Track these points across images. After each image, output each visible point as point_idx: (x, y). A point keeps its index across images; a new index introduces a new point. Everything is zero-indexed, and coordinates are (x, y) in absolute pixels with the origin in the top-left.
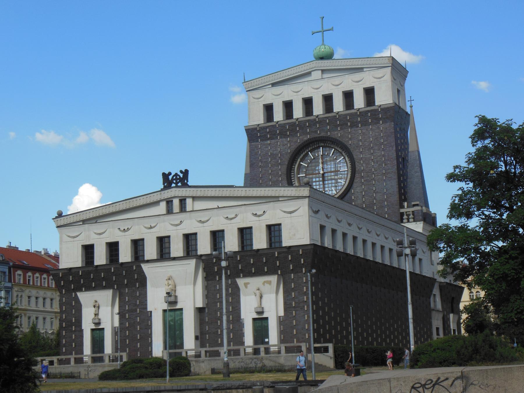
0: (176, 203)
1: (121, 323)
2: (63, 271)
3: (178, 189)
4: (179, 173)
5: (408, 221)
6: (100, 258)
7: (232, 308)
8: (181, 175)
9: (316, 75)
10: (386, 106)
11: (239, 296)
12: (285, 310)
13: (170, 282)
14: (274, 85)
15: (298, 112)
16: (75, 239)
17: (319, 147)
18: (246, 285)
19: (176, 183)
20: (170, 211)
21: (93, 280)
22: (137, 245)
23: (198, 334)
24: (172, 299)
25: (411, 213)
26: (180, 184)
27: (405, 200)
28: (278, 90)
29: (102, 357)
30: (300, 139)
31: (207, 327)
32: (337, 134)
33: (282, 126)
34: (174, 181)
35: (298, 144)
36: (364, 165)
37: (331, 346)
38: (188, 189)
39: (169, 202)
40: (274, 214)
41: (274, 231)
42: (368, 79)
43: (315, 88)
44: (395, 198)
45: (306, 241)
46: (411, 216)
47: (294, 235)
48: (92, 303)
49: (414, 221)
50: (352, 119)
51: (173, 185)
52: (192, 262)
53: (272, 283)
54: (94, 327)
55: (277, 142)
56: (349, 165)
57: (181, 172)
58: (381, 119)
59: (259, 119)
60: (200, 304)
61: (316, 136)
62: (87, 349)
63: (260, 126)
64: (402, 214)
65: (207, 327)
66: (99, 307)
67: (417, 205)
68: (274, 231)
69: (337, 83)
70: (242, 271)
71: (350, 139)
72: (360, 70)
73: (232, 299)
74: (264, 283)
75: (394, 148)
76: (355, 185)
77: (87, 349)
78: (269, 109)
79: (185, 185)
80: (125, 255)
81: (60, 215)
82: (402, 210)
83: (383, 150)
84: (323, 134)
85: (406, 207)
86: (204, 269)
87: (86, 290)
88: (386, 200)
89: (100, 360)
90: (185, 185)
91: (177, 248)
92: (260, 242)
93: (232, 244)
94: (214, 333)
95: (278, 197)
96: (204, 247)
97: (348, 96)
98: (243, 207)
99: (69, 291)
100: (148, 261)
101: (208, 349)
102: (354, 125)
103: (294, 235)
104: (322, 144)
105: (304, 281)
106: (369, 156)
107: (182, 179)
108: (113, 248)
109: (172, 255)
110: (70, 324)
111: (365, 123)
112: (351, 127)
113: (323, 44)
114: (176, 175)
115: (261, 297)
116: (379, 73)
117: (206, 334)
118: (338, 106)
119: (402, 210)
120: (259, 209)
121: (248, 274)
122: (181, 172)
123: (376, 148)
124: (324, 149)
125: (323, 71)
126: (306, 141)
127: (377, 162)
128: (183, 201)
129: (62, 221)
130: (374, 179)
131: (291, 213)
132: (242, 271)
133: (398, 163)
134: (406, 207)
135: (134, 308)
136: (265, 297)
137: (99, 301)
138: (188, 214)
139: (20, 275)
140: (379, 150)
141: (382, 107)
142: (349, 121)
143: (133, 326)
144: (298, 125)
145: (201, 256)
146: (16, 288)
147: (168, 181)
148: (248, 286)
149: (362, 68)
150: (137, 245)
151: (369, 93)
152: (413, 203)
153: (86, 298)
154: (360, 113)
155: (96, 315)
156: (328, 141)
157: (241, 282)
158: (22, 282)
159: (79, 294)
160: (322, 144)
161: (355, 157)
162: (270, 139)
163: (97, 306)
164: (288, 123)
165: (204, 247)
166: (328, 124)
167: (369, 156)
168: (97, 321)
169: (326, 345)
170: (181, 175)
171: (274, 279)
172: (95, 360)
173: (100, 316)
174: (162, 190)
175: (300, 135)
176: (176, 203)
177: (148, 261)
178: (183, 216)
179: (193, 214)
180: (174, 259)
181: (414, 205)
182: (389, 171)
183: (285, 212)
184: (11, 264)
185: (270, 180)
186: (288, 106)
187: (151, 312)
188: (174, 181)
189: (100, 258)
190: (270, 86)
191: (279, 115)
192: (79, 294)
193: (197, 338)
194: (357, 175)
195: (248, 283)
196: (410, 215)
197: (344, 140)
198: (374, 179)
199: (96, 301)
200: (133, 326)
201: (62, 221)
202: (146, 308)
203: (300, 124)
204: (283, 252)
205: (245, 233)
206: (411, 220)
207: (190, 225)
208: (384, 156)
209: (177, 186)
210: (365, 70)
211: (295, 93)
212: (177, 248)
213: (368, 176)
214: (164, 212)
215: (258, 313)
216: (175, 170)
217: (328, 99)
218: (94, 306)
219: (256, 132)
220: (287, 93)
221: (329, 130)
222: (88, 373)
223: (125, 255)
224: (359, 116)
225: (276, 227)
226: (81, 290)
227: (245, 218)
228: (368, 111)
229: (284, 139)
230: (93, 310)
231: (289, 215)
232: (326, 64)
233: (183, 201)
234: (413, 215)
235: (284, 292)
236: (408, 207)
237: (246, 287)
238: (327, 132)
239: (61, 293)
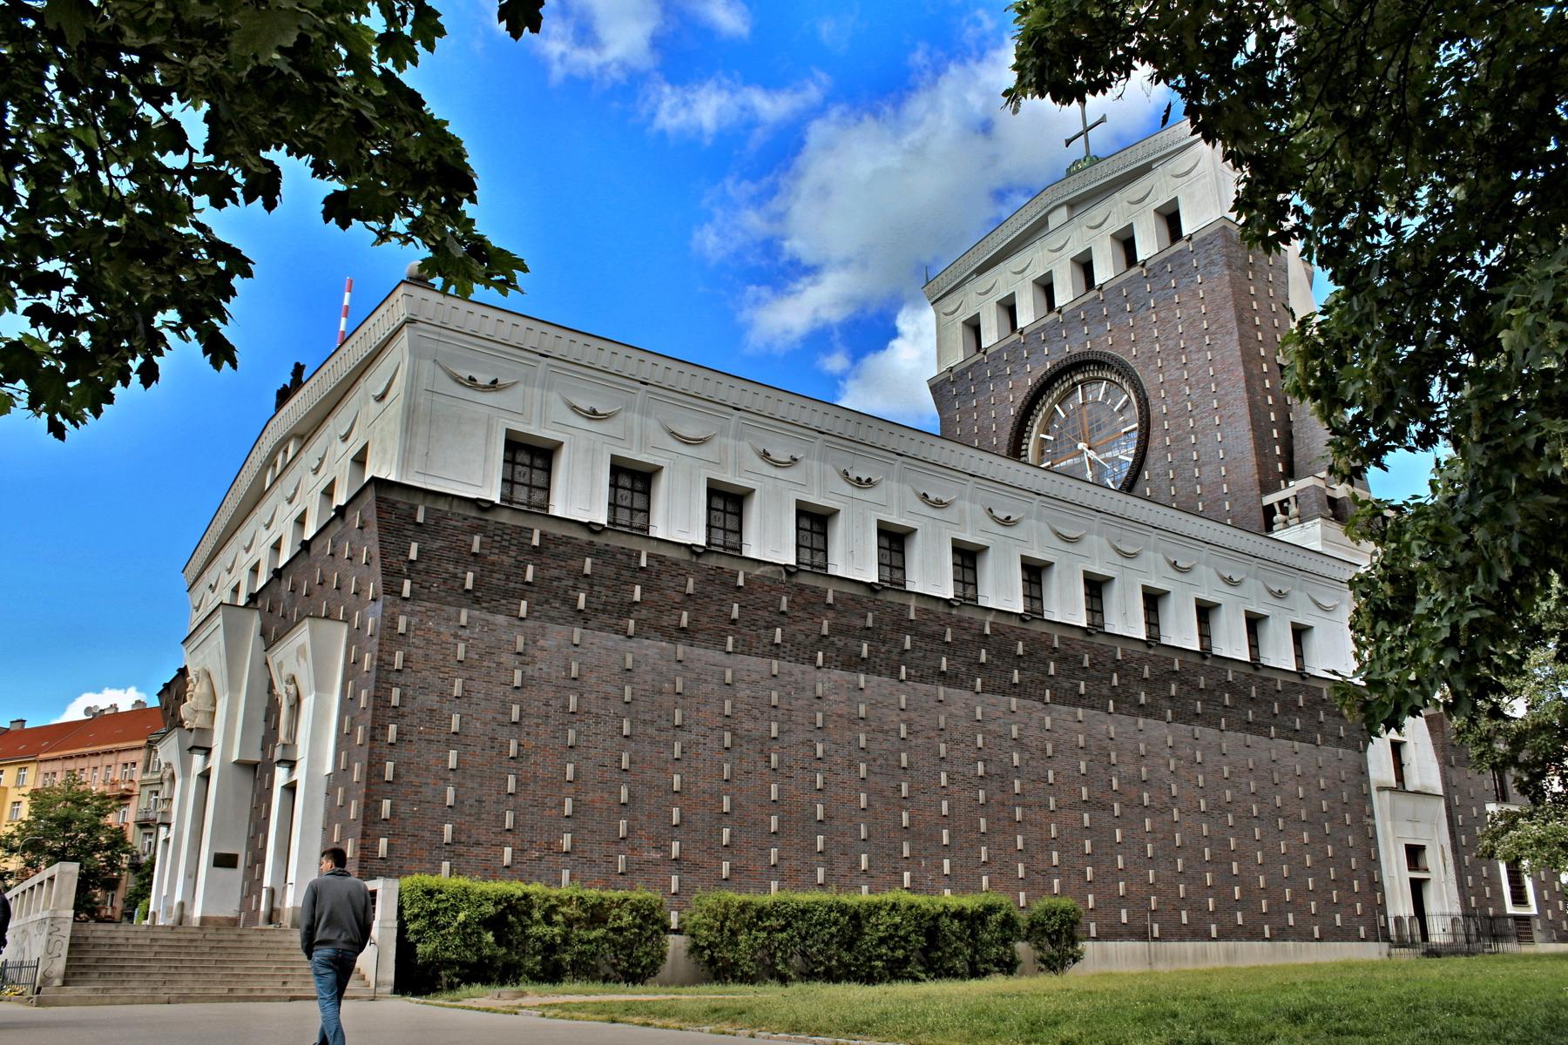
5: (1286, 524)
9: (1055, 220)
10: (1204, 234)
17: (1075, 385)
64: (1269, 511)
72: (1146, 169)
75: (1236, 336)
76: (1152, 456)
82: (1269, 499)
84: (1076, 351)
123: (1193, 348)
125: (1072, 205)
151: (1171, 218)
167: (1178, 373)
194: (1155, 432)
213: (1179, 426)
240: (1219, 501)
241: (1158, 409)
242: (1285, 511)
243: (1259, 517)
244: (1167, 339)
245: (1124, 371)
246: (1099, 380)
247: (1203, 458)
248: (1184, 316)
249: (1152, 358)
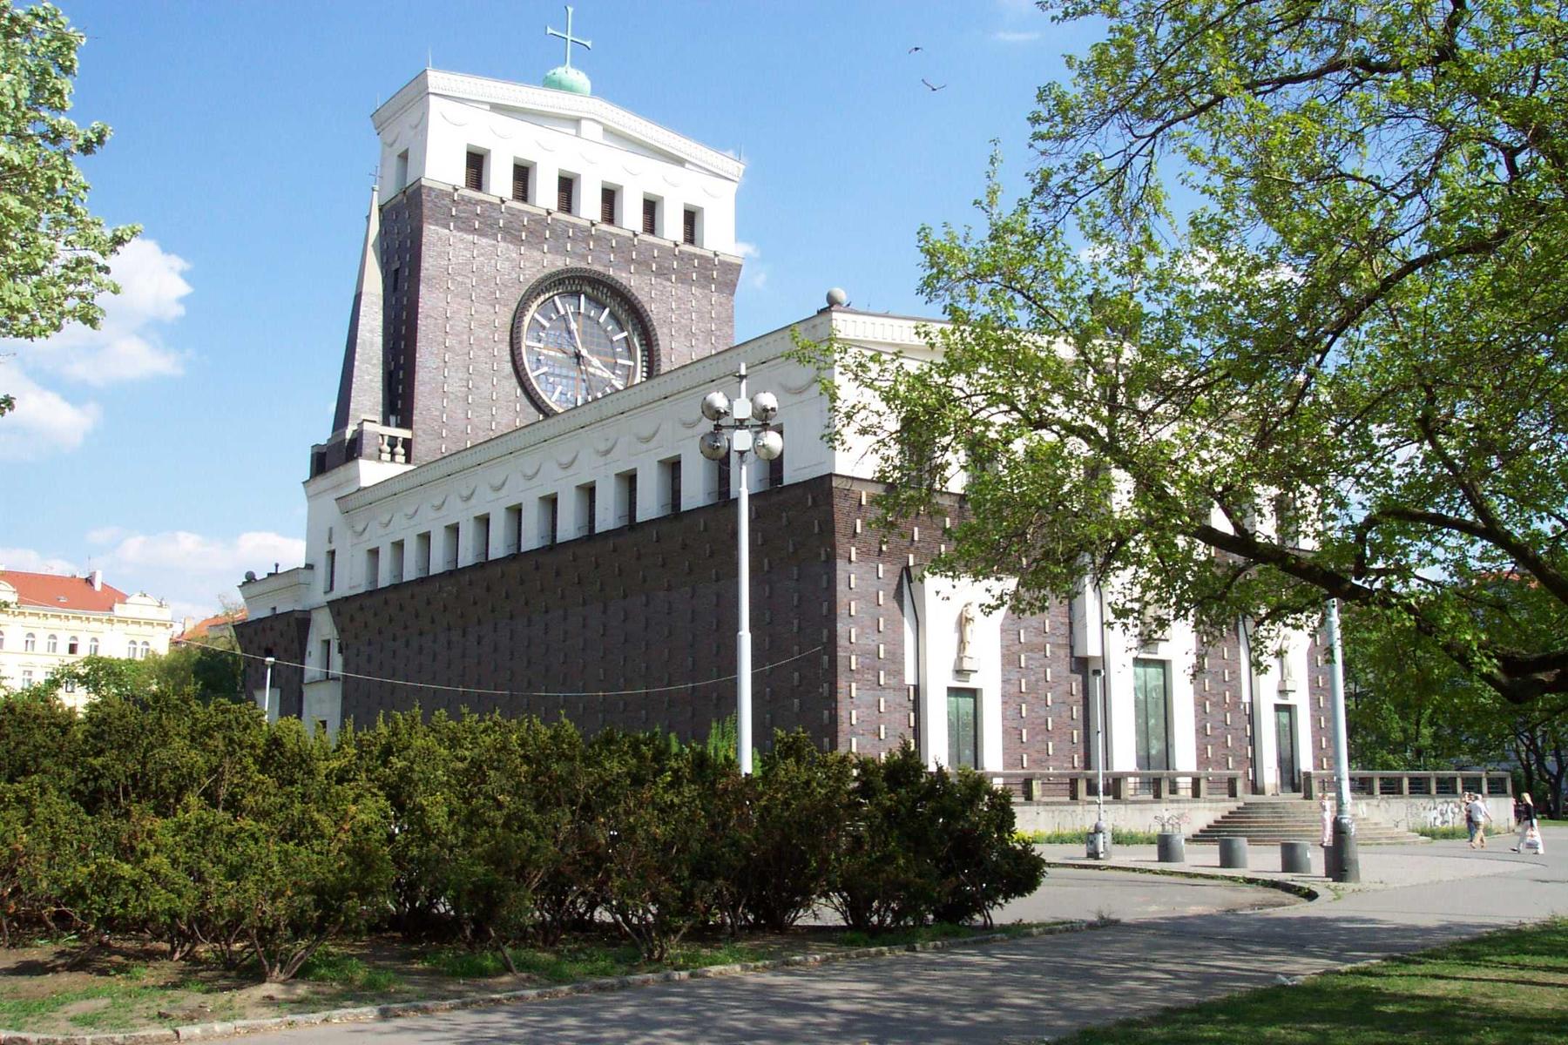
10: (728, 259)
14: (496, 108)
56: (639, 353)
72: (681, 162)
84: (598, 268)
102: (662, 273)
111: (684, 279)
160: (589, 290)
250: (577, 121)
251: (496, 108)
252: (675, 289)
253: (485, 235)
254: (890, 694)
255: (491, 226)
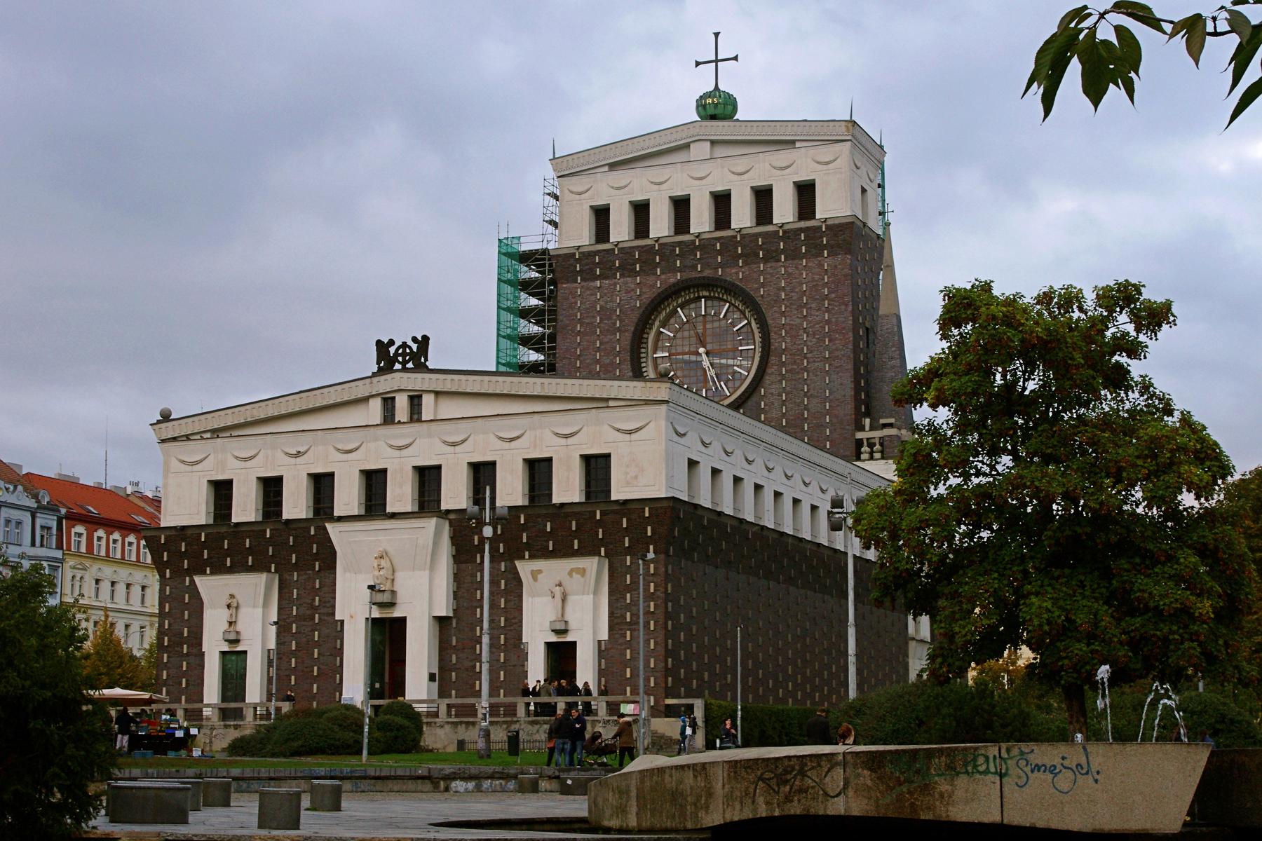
0: (402, 402)
1: (279, 643)
2: (168, 533)
3: (406, 375)
4: (410, 343)
5: (872, 458)
6: (246, 509)
7: (506, 620)
8: (415, 347)
10: (837, 222)
11: (520, 596)
12: (611, 628)
13: (383, 563)
14: (613, 166)
15: (661, 225)
16: (195, 468)
17: (699, 298)
18: (535, 574)
19: (404, 363)
20: (389, 418)
21: (228, 553)
22: (322, 484)
23: (436, 670)
24: (383, 597)
25: (877, 441)
26: (410, 365)
27: (868, 414)
28: (621, 176)
29: (241, 709)
30: (660, 281)
31: (454, 657)
32: (737, 273)
33: (626, 252)
34: (400, 359)
35: (656, 291)
36: (788, 340)
37: (699, 705)
38: (427, 376)
39: (389, 403)
40: (596, 434)
41: (596, 468)
42: (803, 165)
43: (698, 179)
44: (848, 409)
45: (659, 491)
46: (878, 447)
47: (636, 477)
48: (226, 600)
49: (883, 458)
50: (769, 245)
51: (398, 366)
52: (431, 523)
53: (588, 572)
54: (227, 649)
55: (615, 285)
56: (758, 339)
57: (414, 339)
58: (825, 247)
59: (580, 235)
60: (443, 608)
61: (694, 275)
62: (212, 692)
63: (581, 250)
64: (859, 443)
65: (454, 657)
66: (237, 608)
67: (891, 425)
68: (596, 468)
69: (740, 169)
70: (528, 546)
71: (763, 285)
72: (791, 143)
73: (506, 602)
74: (570, 574)
75: (850, 308)
76: (768, 379)
77: (212, 692)
78: (601, 215)
79: (421, 367)
80: (296, 505)
81: (166, 417)
82: (859, 435)
83: (827, 310)
84: (707, 273)
85: (867, 428)
86: (454, 539)
87: (212, 573)
88: (828, 412)
89: (238, 714)
90: (421, 367)
91: (400, 495)
92: (567, 488)
93: (511, 490)
94: (467, 669)
95: (607, 400)
96: (455, 494)
97: (763, 197)
98: (536, 416)
99: (179, 573)
100: (340, 519)
101: (453, 700)
102: (771, 257)
103: (636, 477)
104: (706, 293)
105: (652, 571)
106: (798, 321)
107: (416, 354)
108: (272, 488)
109: (389, 510)
110: (178, 640)
111: (793, 255)
112: (766, 260)
113: (716, 87)
114: (404, 345)
115: (564, 600)
116: (826, 152)
117: (451, 670)
118: (742, 215)
119: (859, 435)
120: (567, 423)
121: (541, 553)
122: (414, 339)
124: (709, 303)
125: (713, 142)
126: (674, 285)
127: (814, 334)
128: (415, 401)
129: (169, 430)
130: (805, 369)
131: (631, 432)
132: (528, 546)
133: (856, 338)
134: (867, 428)
135: (308, 612)
136: (571, 599)
137: (238, 597)
138: (425, 425)
139: (80, 535)
140: (819, 310)
141: (829, 222)
142: (761, 248)
143: (305, 647)
144: (657, 252)
145: (448, 512)
146: (71, 562)
147: (387, 356)
148: (539, 576)
149: (793, 142)
150: (322, 484)
151: (806, 192)
152: (882, 421)
153: (212, 588)
154: (784, 232)
155: (231, 623)
156: (717, 287)
157: (524, 568)
158: (83, 549)
159: (197, 579)
160: (706, 293)
161: (770, 322)
162: (602, 277)
163: (232, 606)
164: (638, 247)
165: (455, 494)
166: (720, 252)
167: (798, 321)
168: (232, 637)
169: (689, 701)
170: (415, 347)
171: (591, 564)
172: (225, 714)
173: (239, 627)
174: (374, 375)
175: (662, 273)
176: (402, 402)
177: (340, 519)
178: (415, 427)
179: (434, 426)
180: (394, 516)
181: (885, 426)
182: (837, 353)
183: (619, 430)
184: (63, 511)
185: (598, 362)
186: (641, 211)
187: (342, 622)
188: (400, 359)
189: (246, 509)
190: (606, 168)
191: (621, 230)
192: (197, 579)
193: (432, 677)
194: (773, 360)
195: (540, 571)
196: (875, 445)
197: (748, 287)
198: (805, 369)
199: (232, 596)
200: (305, 647)
201: (169, 430)
202: (333, 614)
203: (665, 249)
204: (613, 512)
205: (539, 470)
206: (877, 455)
207: (426, 448)
208: (828, 322)
209: (404, 369)
210: (798, 145)
211: (657, 186)
212: (400, 495)
214: (377, 419)
215: (558, 632)
216: (402, 335)
217: (722, 201)
218: (229, 606)
219: (572, 261)
220: (639, 183)
221: (721, 265)
222: (211, 742)
223: (296, 505)
224: (782, 238)
225: (599, 460)
226: (204, 573)
227: (540, 443)
228: (801, 230)
229: (629, 279)
230: (225, 615)
231: (627, 437)
232: (720, 129)
233: (415, 401)
234: (881, 445)
235: (611, 593)
236: (872, 429)
237: (535, 579)
238: (716, 269)
239: (162, 576)
240: (822, 426)
241: (781, 342)
242: (871, 445)
243: (853, 446)
244: (792, 291)
245: (751, 304)
246: (726, 301)
247: (812, 392)
248: (809, 278)
249: (778, 301)
250: (686, 146)
251: (613, 166)
252: (782, 267)
253: (606, 278)
254: (192, 659)
255: (611, 269)
